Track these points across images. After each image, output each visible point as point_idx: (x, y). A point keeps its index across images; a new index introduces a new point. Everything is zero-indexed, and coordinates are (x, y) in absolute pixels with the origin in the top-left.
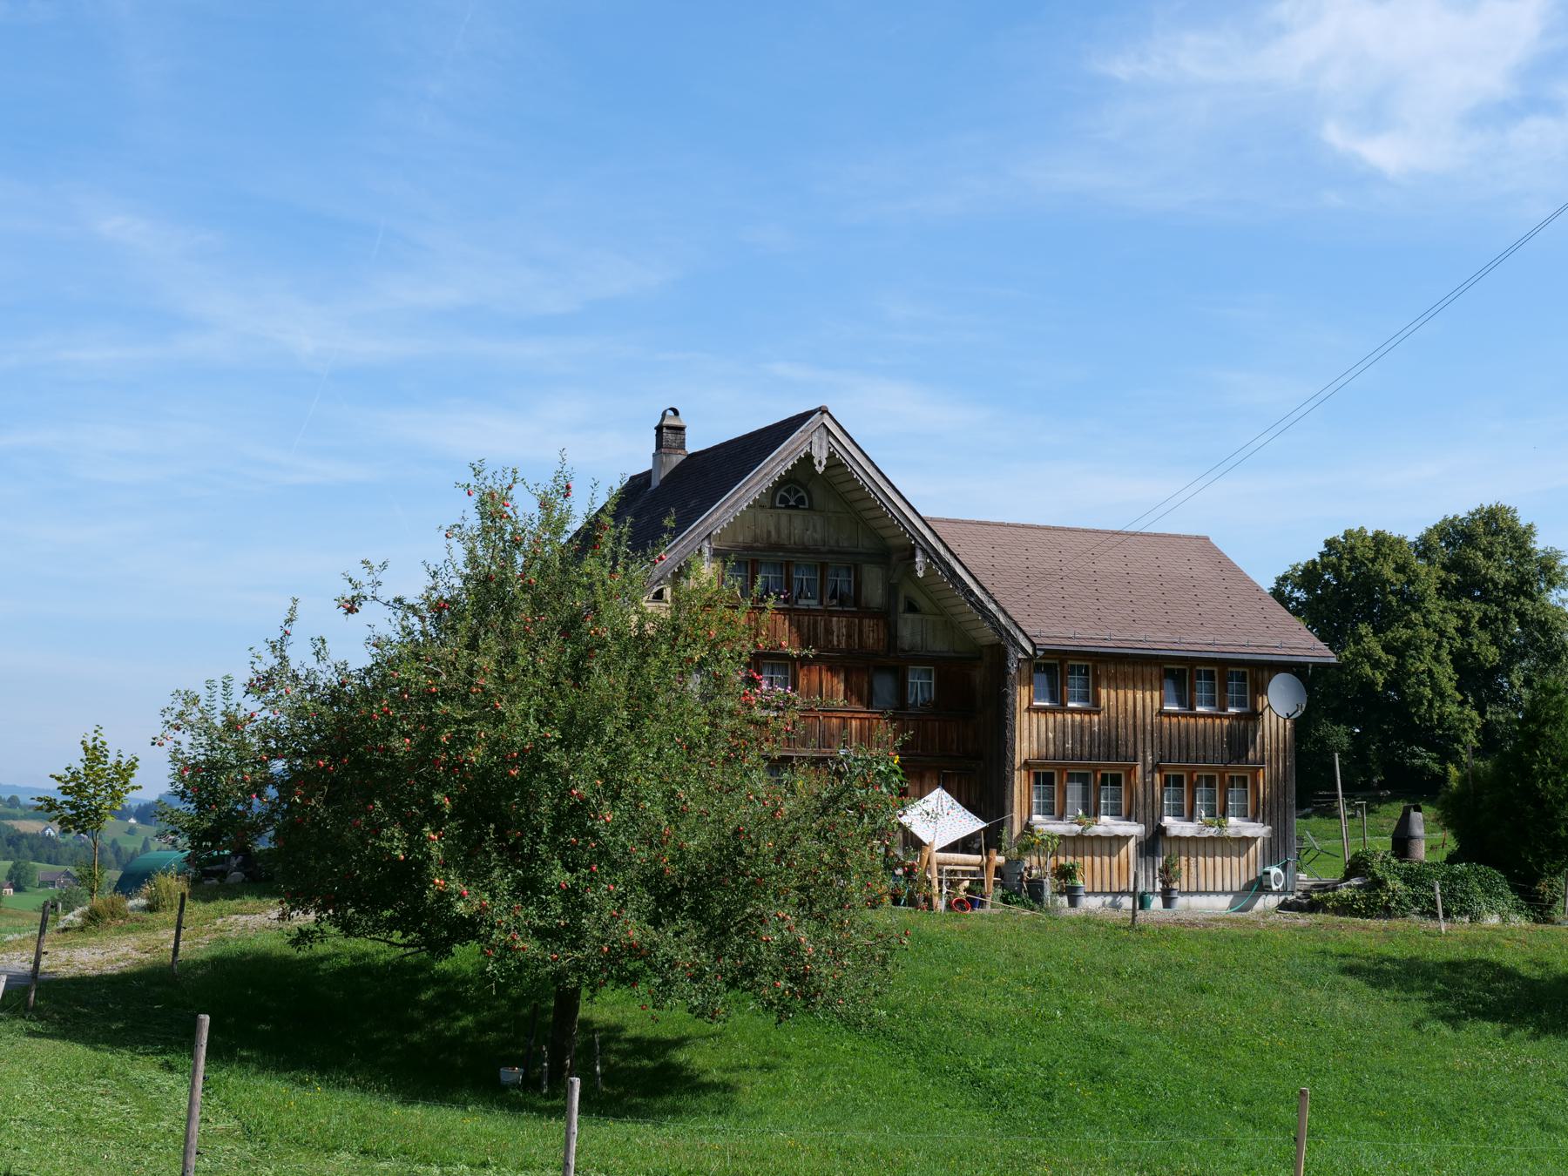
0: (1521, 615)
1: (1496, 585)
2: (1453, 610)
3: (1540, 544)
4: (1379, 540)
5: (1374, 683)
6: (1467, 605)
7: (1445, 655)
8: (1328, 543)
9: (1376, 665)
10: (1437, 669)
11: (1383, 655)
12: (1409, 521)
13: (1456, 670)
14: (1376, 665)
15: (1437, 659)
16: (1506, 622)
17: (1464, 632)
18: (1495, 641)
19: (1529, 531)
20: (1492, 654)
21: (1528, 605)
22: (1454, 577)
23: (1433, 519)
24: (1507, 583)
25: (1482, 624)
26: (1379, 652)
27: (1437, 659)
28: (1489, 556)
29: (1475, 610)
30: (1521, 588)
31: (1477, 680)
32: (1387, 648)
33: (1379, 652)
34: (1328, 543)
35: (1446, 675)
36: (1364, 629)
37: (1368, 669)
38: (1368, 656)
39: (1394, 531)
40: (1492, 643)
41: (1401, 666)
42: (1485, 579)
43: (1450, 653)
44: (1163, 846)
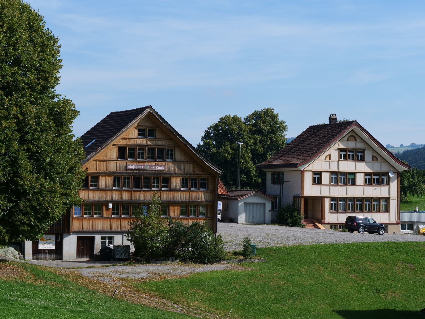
0: (271, 139)
1: (265, 131)
2: (252, 138)
3: (280, 118)
4: (234, 118)
5: (227, 158)
6: (256, 136)
7: (249, 150)
8: (220, 119)
9: (229, 153)
10: (246, 154)
11: (231, 151)
12: (243, 114)
13: (252, 154)
14: (229, 153)
15: (246, 151)
16: (267, 141)
17: (255, 144)
18: (263, 146)
19: (277, 116)
20: (261, 150)
21: (273, 137)
22: (254, 129)
23: (252, 112)
24: (269, 130)
25: (260, 142)
26: (230, 150)
27: (246, 151)
28: (264, 122)
29: (258, 137)
30: (273, 131)
31: (257, 157)
32: (232, 149)
33: (230, 150)
34: (220, 119)
35: (248, 156)
36: (227, 143)
37: (226, 154)
38: (227, 151)
39: (238, 116)
40: (262, 147)
41: (235, 154)
42: (262, 129)
43: (251, 150)
44: (83, 183)
